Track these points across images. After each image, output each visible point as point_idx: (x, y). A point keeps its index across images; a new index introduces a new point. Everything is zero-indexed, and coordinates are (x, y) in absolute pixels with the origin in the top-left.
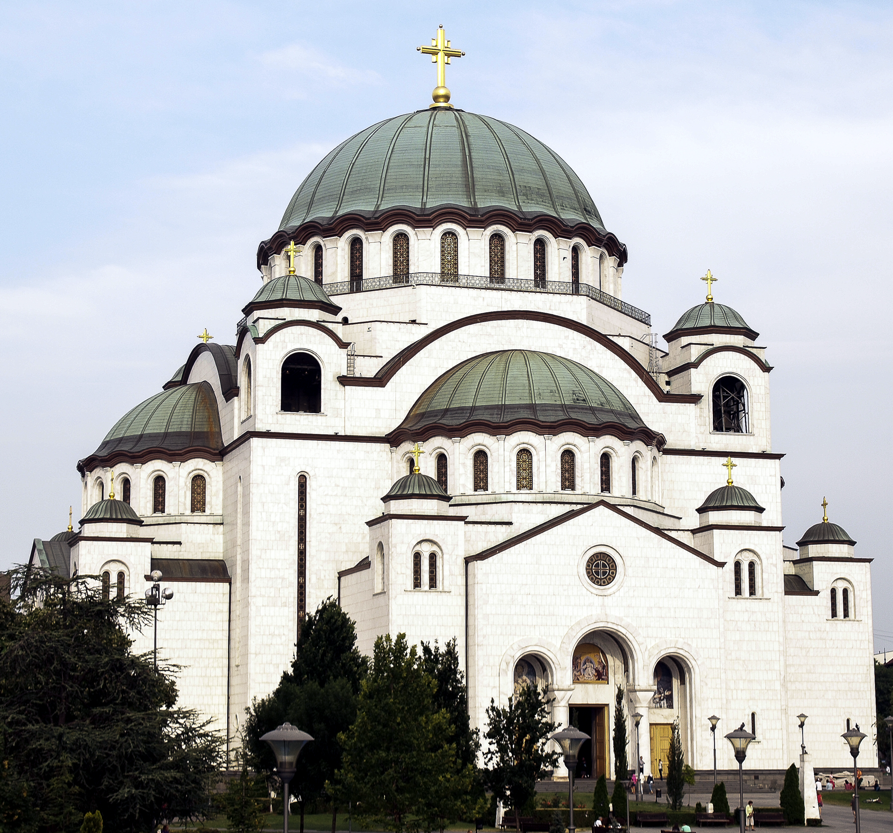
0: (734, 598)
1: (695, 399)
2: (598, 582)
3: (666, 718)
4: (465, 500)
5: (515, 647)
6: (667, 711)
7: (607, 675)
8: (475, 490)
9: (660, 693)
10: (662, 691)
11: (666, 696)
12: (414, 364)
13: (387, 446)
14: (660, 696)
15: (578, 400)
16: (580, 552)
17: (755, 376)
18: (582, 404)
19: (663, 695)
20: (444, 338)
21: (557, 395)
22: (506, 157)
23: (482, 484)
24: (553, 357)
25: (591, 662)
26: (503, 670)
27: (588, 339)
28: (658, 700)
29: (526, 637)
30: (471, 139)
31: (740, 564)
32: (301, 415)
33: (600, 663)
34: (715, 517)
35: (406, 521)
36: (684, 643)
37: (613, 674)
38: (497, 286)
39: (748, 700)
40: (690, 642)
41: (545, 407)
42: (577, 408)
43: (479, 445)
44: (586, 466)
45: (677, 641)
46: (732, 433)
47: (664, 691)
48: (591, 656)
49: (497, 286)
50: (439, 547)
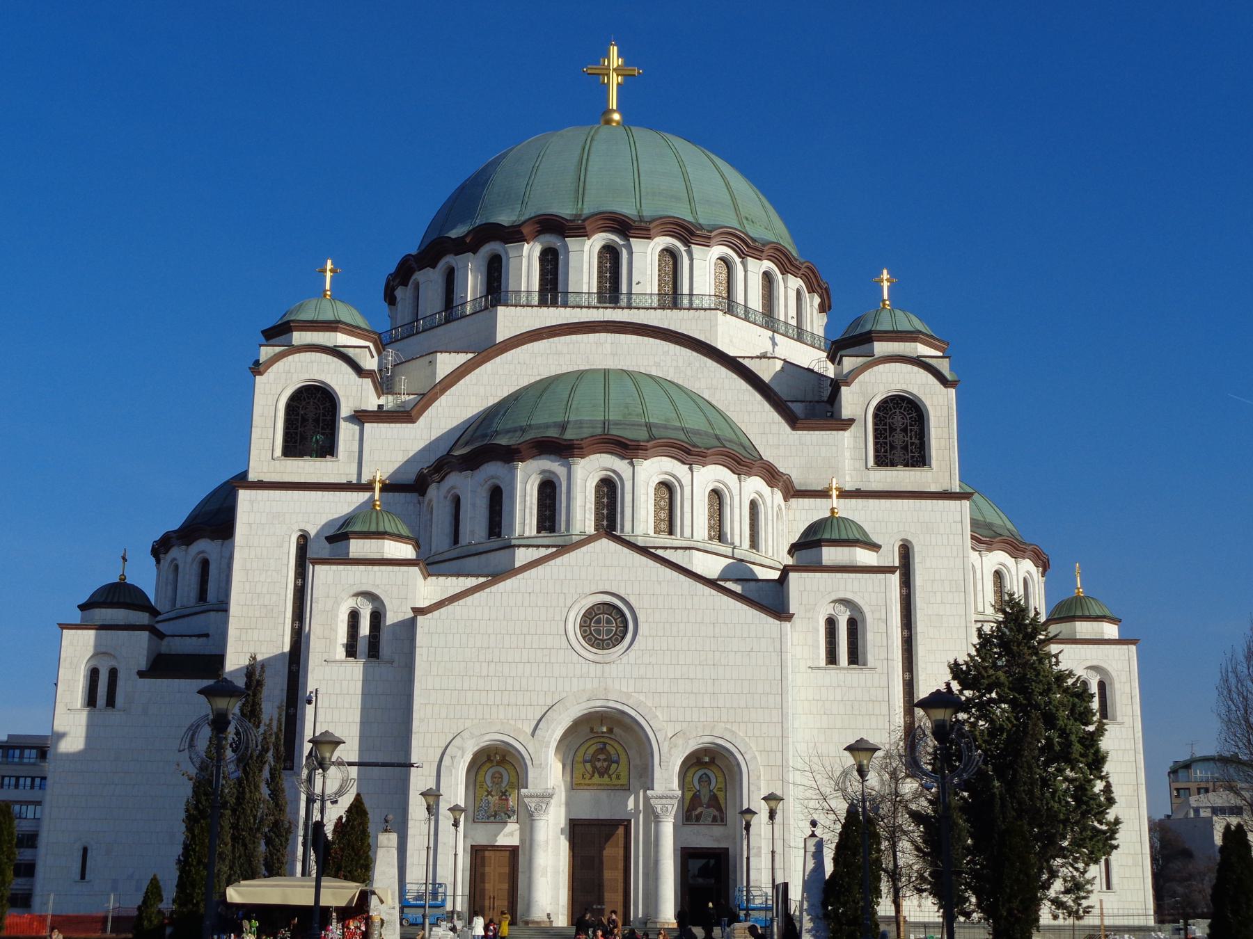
0: (819, 668)
1: (846, 424)
2: (598, 645)
4: (473, 549)
6: (717, 830)
8: (489, 539)
12: (457, 394)
13: (413, 497)
15: (630, 414)
18: (635, 419)
20: (498, 359)
21: (602, 409)
22: (635, 158)
23: (497, 530)
24: (657, 382)
26: (446, 767)
27: (695, 354)
29: (484, 721)
30: (595, 143)
31: (832, 619)
32: (305, 461)
36: (726, 729)
38: (602, 305)
41: (580, 424)
42: (624, 424)
43: (493, 477)
44: (628, 498)
45: (713, 728)
46: (900, 467)
49: (602, 305)
50: (382, 603)
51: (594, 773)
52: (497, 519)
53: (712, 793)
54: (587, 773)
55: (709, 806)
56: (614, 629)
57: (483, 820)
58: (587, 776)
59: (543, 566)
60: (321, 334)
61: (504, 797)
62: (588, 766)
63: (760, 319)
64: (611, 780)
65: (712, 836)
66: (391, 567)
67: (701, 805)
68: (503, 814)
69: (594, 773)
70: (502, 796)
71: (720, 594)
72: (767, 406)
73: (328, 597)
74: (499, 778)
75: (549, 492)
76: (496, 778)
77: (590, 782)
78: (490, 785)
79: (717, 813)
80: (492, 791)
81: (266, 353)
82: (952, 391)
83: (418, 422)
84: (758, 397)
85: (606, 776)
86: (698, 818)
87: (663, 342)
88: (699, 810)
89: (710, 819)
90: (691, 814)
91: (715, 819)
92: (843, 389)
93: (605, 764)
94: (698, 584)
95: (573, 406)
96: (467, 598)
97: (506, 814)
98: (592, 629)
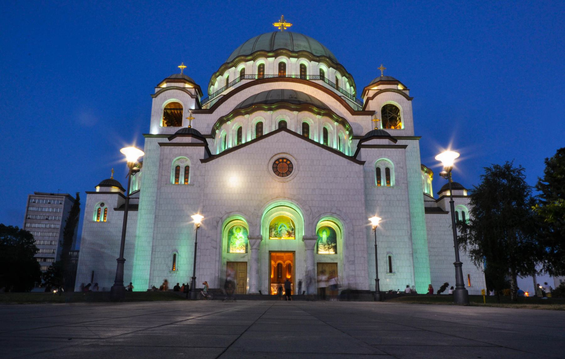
5: (223, 212)
7: (295, 234)
9: (329, 245)
10: (330, 243)
11: (333, 246)
14: (328, 246)
16: (269, 158)
17: (404, 102)
18: (293, 99)
19: (330, 246)
25: (284, 227)
27: (315, 89)
28: (327, 248)
33: (290, 227)
34: (363, 144)
35: (169, 147)
37: (298, 233)
39: (386, 248)
40: (341, 209)
45: (332, 209)
47: (331, 243)
48: (284, 224)
52: (240, 135)
56: (288, 169)
59: (257, 142)
60: (177, 84)
63: (335, 86)
66: (193, 147)
71: (333, 153)
72: (342, 106)
73: (167, 159)
75: (259, 126)
81: (157, 90)
82: (410, 102)
83: (213, 114)
84: (339, 103)
87: (303, 85)
92: (370, 101)
94: (323, 149)
95: (270, 96)
96: (224, 156)
98: (278, 169)
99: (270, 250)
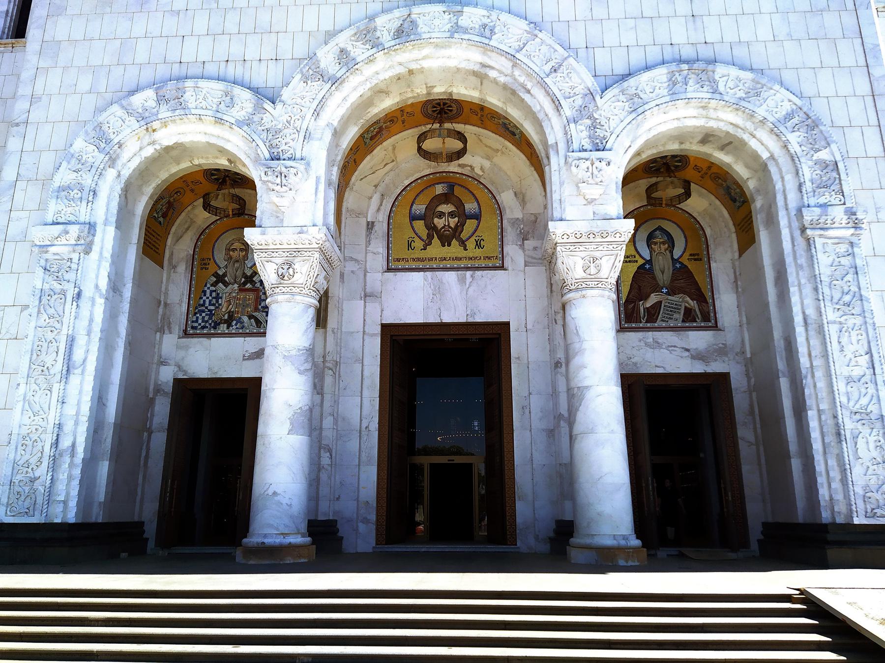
3: (698, 356)
51: (430, 237)
53: (678, 265)
54: (417, 239)
55: (672, 292)
57: (205, 331)
58: (419, 244)
61: (249, 286)
62: (420, 225)
64: (466, 249)
65: (687, 350)
67: (657, 288)
68: (245, 319)
69: (430, 237)
70: (245, 284)
74: (241, 250)
76: (234, 250)
77: (423, 254)
78: (223, 264)
79: (693, 304)
80: (225, 275)
85: (454, 242)
86: (653, 314)
88: (653, 299)
89: (680, 316)
90: (636, 309)
91: (689, 316)
93: (453, 222)
97: (251, 317)
99: (384, 322)
